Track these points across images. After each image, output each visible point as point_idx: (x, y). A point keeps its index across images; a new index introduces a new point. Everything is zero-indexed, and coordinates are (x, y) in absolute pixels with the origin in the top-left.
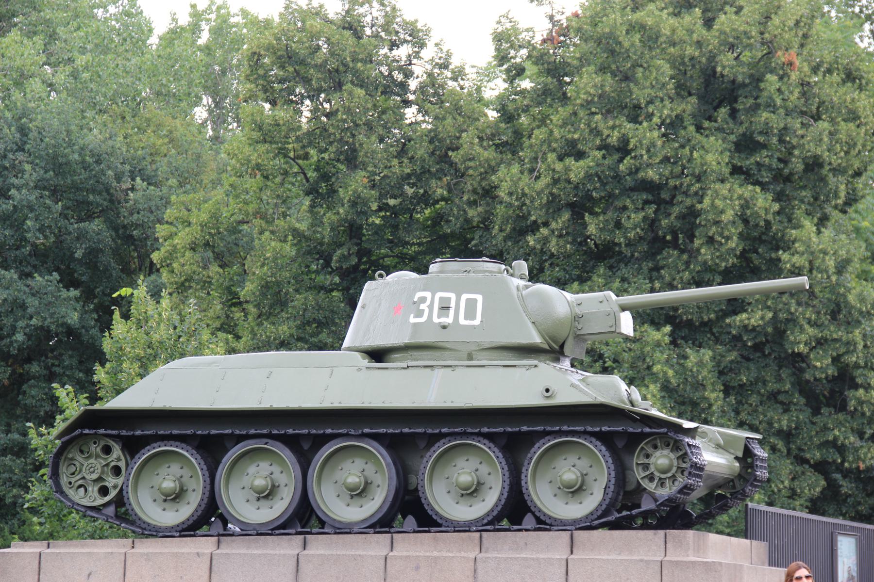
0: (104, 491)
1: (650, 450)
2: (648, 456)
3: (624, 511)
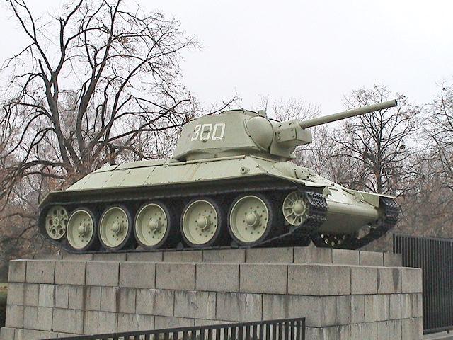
3: (279, 236)
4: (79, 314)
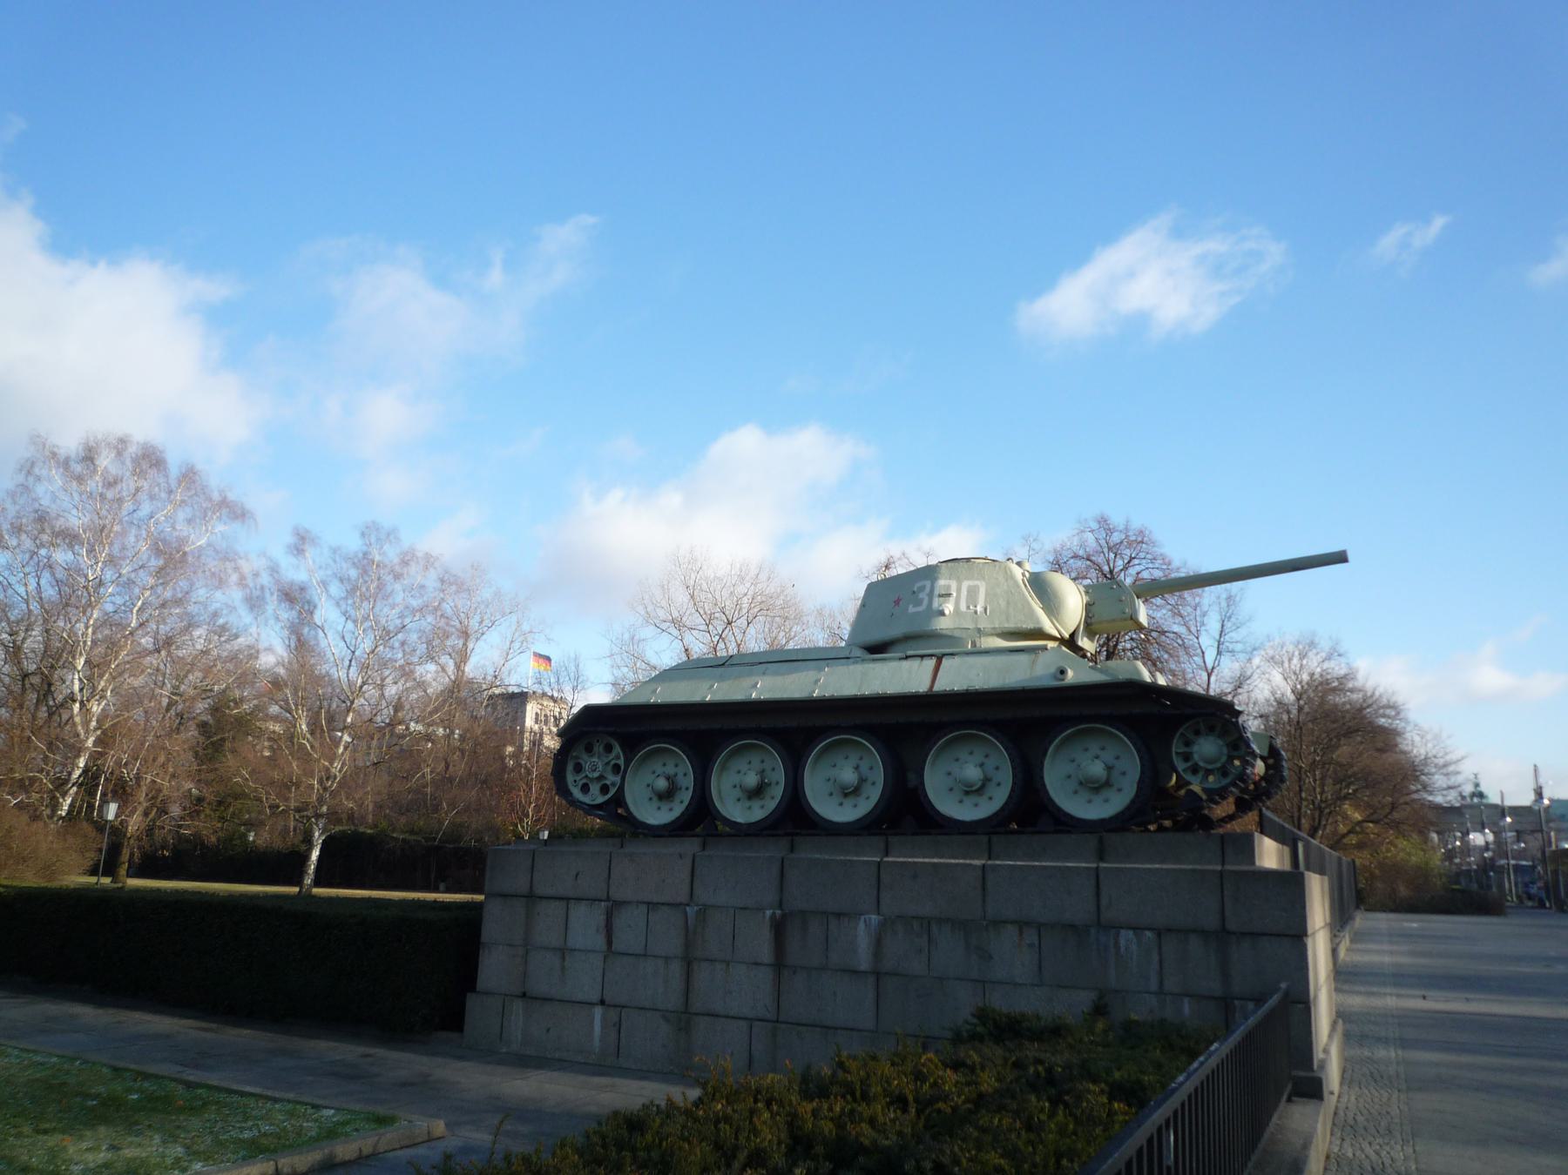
0: (605, 789)
1: (1191, 736)
2: (1188, 744)
4: (676, 968)
